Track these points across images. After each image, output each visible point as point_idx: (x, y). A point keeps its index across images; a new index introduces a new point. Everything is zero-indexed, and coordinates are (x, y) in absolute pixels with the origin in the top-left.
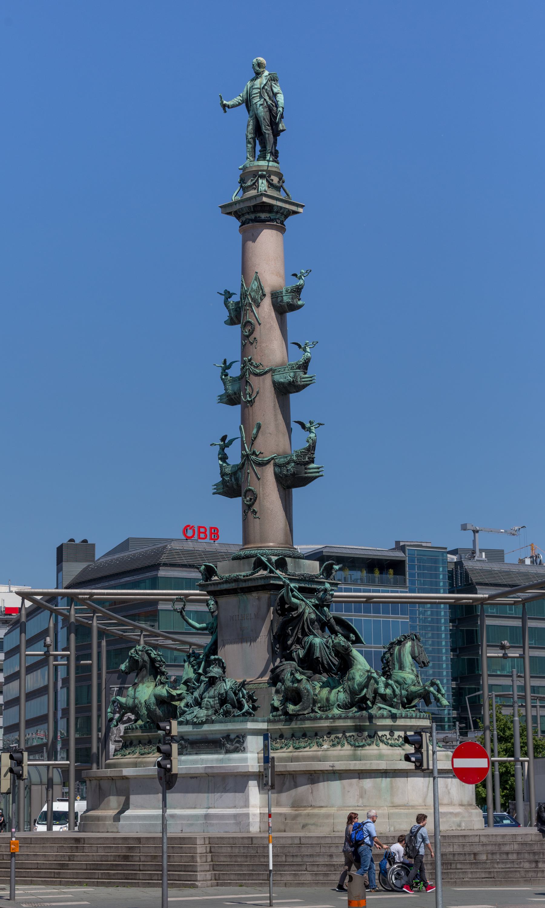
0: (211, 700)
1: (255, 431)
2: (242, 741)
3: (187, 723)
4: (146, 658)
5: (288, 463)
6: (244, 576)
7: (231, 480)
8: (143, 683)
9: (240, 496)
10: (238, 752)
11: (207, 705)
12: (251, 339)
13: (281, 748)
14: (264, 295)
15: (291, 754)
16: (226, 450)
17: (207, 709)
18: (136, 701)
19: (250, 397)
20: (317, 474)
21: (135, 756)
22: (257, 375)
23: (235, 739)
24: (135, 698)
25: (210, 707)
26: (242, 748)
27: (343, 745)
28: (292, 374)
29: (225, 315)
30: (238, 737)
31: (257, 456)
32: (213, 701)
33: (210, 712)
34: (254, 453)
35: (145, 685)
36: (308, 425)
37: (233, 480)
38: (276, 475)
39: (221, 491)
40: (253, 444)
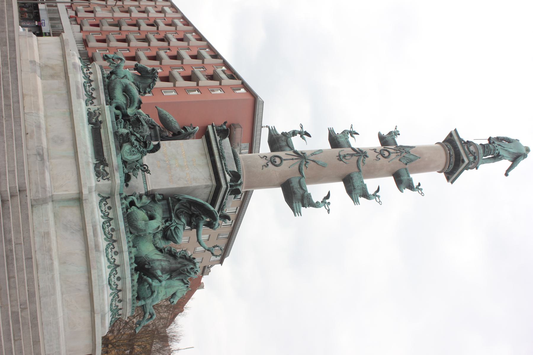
2: (104, 178)
5: (302, 189)
6: (225, 164)
9: (272, 150)
10: (97, 175)
12: (380, 156)
13: (102, 211)
14: (406, 164)
15: (98, 223)
16: (299, 135)
20: (295, 210)
21: (82, 78)
22: (358, 161)
23: (105, 171)
27: (109, 267)
29: (385, 133)
30: (107, 174)
34: (307, 162)
36: (327, 201)
39: (272, 132)
40: (313, 161)
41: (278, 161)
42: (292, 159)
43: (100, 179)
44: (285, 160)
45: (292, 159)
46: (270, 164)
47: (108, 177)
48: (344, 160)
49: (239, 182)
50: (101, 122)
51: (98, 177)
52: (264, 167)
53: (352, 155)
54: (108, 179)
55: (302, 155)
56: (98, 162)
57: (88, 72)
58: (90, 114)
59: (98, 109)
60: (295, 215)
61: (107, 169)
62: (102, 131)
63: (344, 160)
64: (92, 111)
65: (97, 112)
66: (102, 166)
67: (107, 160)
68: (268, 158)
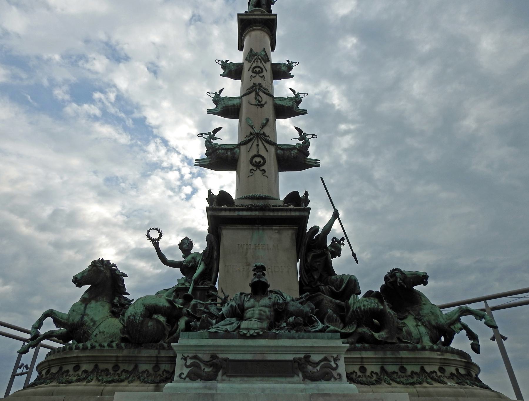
0: (267, 310)
1: (265, 122)
3: (227, 335)
4: (108, 274)
6: (273, 206)
7: (227, 153)
8: (97, 301)
10: (328, 380)
11: (260, 314)
12: (261, 75)
17: (260, 319)
18: (86, 318)
19: (259, 102)
24: (83, 315)
25: (264, 317)
26: (335, 375)
28: (291, 103)
31: (265, 136)
32: (270, 311)
33: (265, 325)
34: (264, 134)
35: (99, 303)
37: (229, 153)
38: (277, 155)
41: (258, 159)
42: (258, 145)
43: (335, 373)
44: (258, 151)
45: (258, 145)
46: (262, 168)
47: (332, 360)
48: (263, 102)
49: (301, 195)
50: (214, 357)
51: (333, 376)
52: (265, 174)
53: (257, 94)
54: (335, 360)
55: (252, 137)
56: (301, 375)
57: (71, 372)
58: (193, 376)
59: (185, 359)
60: (319, 166)
61: (316, 358)
62: (231, 357)
63: (263, 102)
64: (186, 371)
65: (189, 362)
66: (310, 368)
67: (298, 356)
68: (254, 168)
